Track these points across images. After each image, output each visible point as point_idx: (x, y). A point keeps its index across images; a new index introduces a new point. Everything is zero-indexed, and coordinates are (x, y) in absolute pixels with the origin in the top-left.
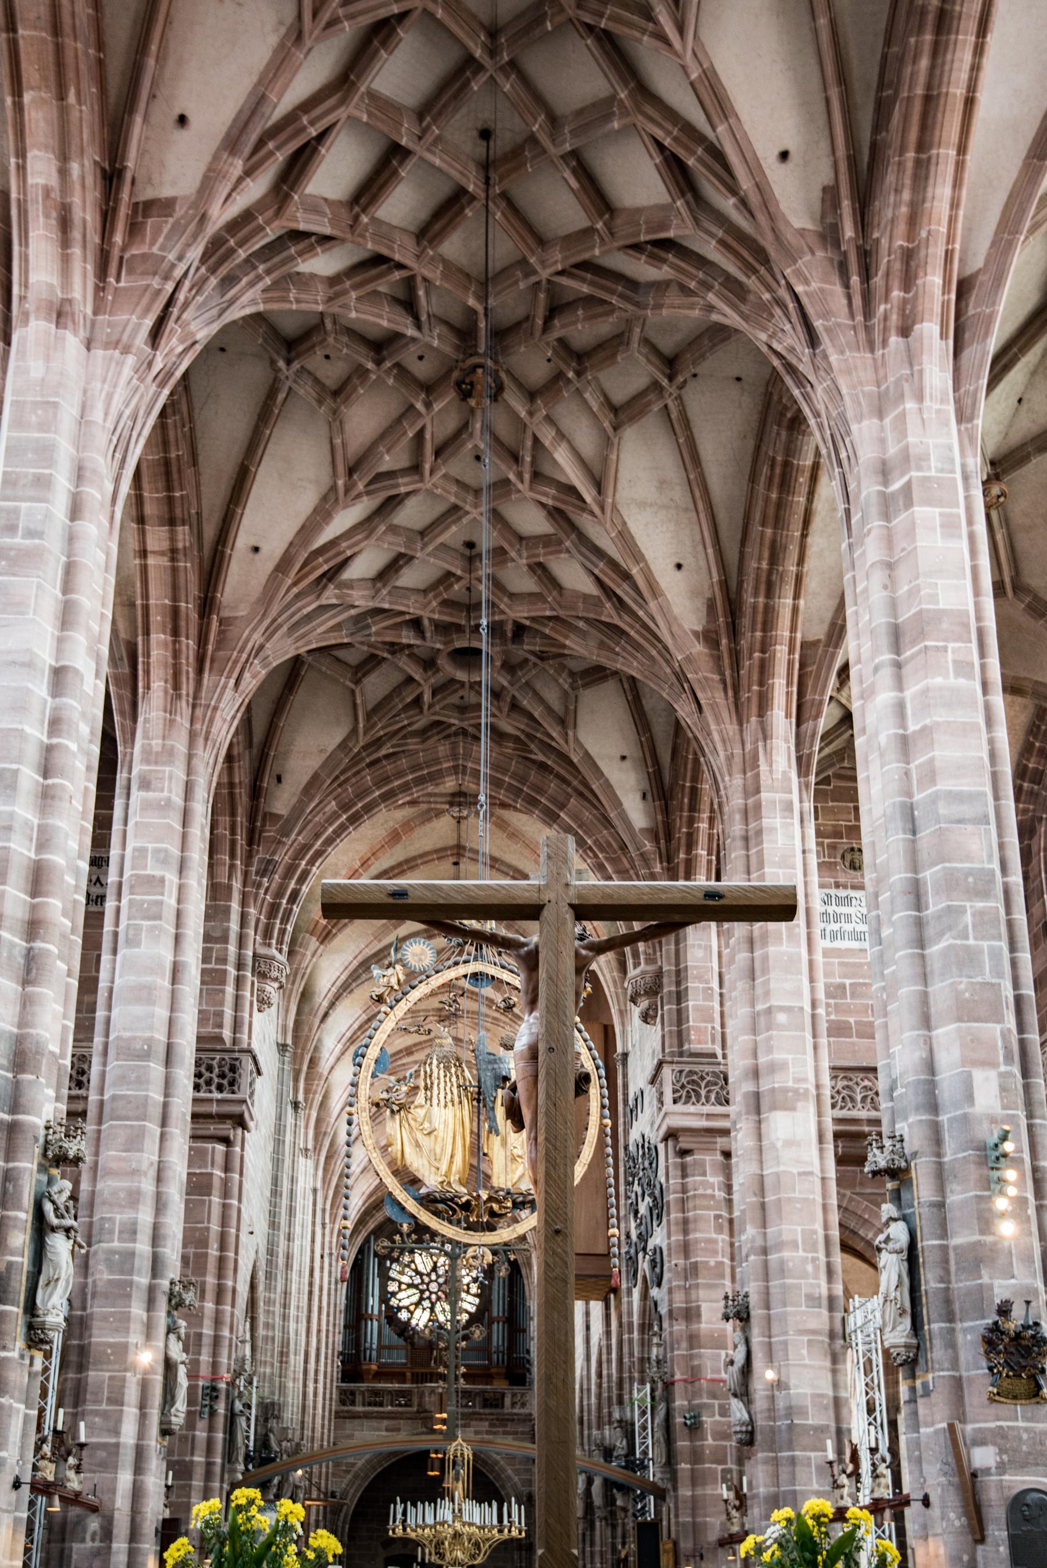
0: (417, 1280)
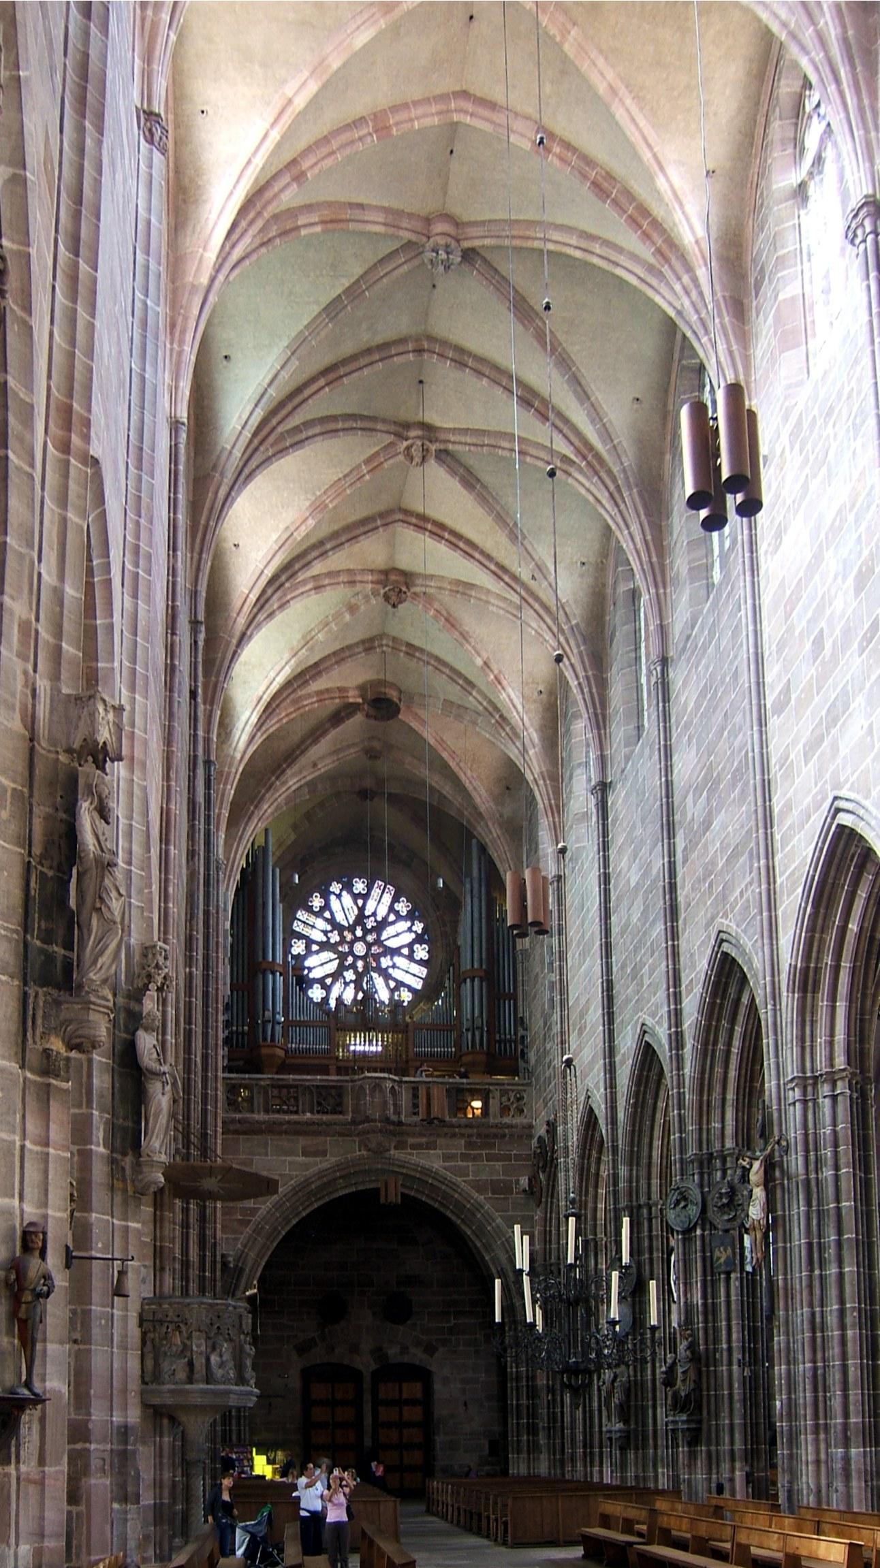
0: (335, 937)
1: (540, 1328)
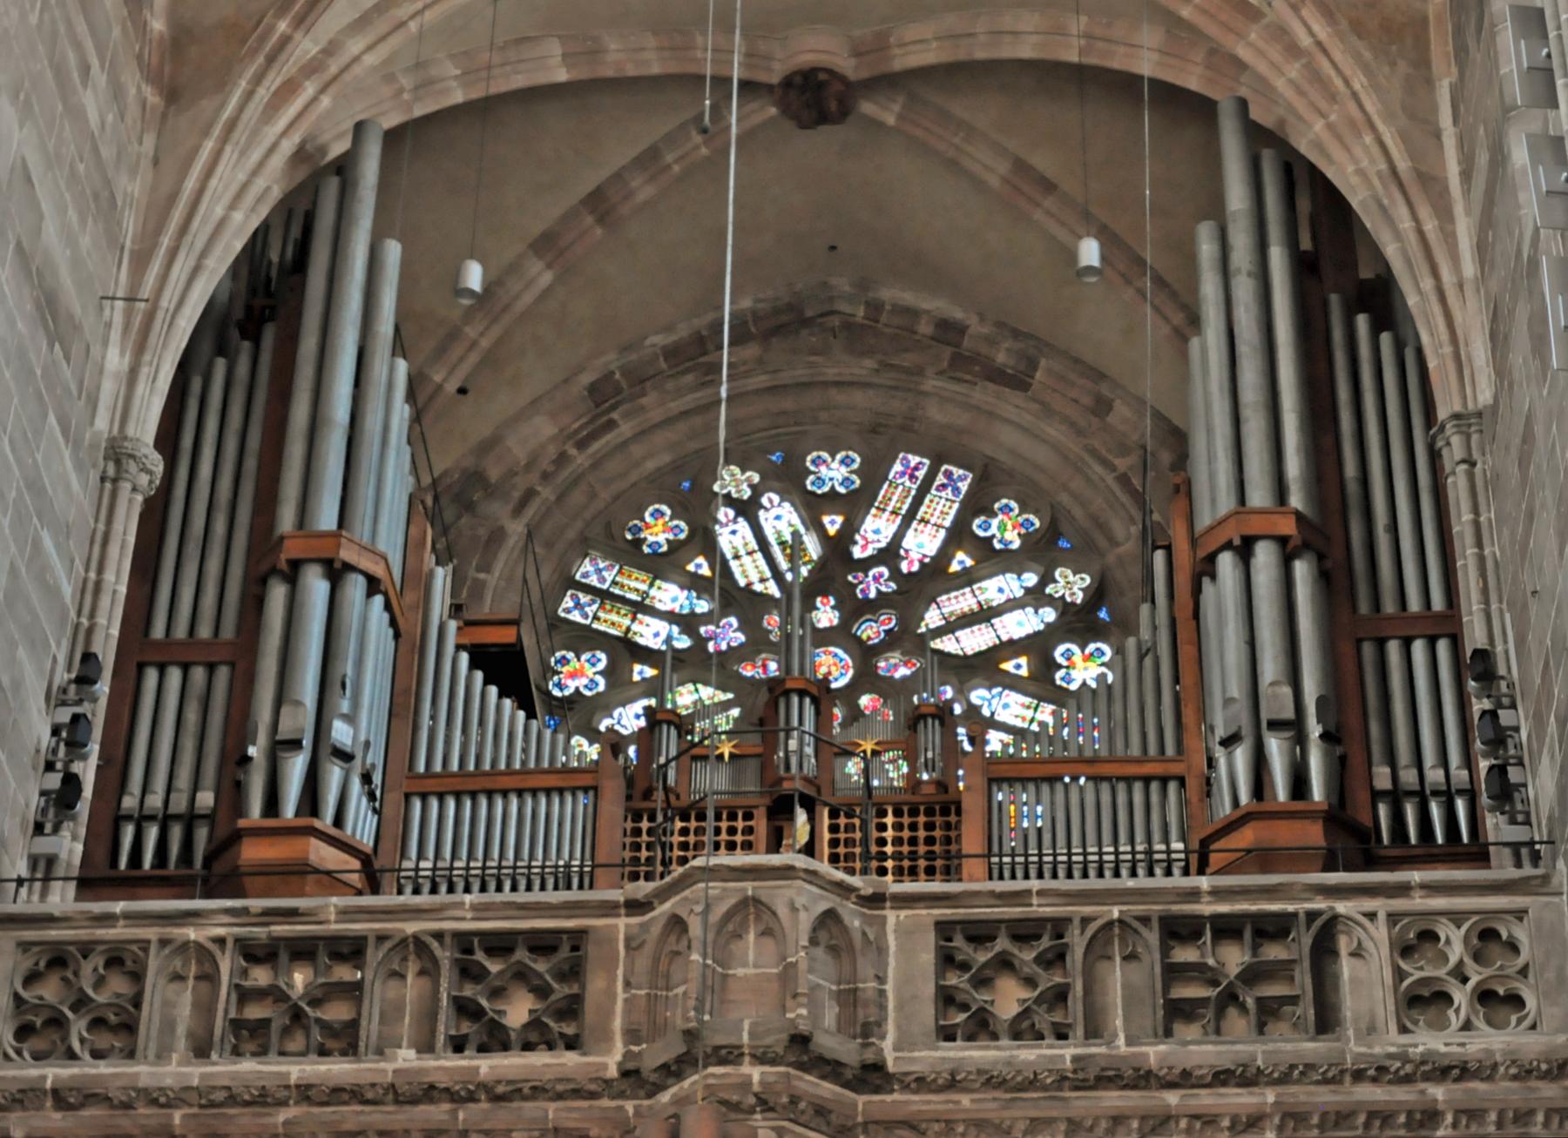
1: (1334, 300)
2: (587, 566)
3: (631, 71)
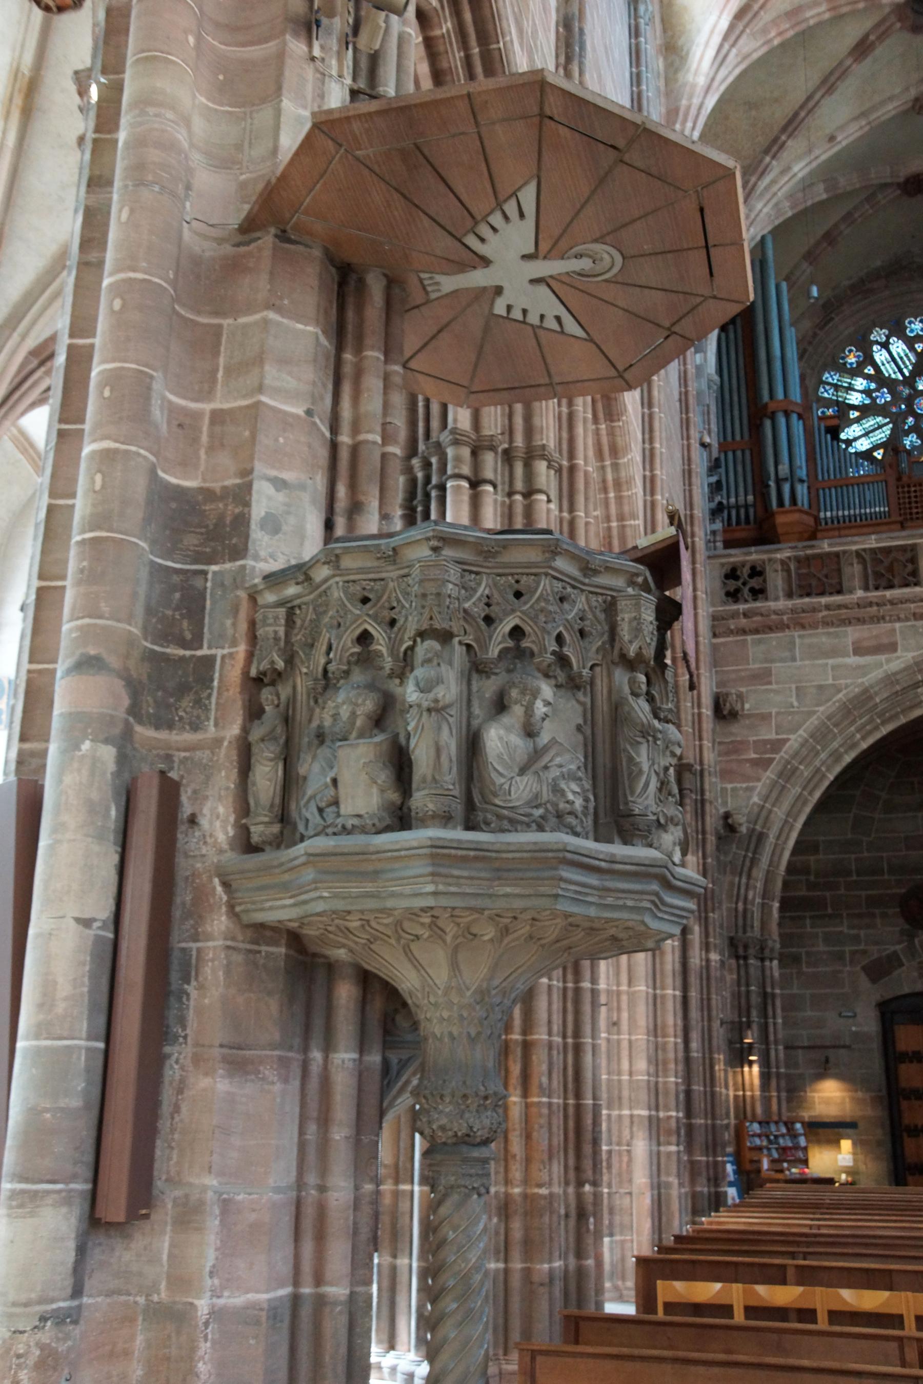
2: (827, 375)
3: (849, 189)
